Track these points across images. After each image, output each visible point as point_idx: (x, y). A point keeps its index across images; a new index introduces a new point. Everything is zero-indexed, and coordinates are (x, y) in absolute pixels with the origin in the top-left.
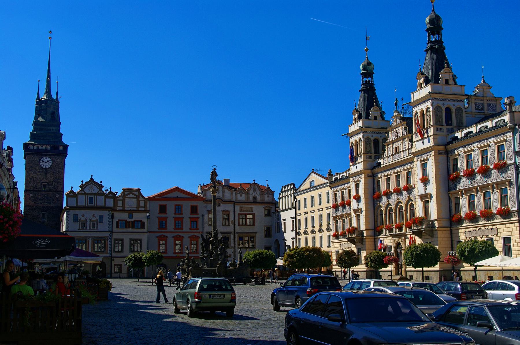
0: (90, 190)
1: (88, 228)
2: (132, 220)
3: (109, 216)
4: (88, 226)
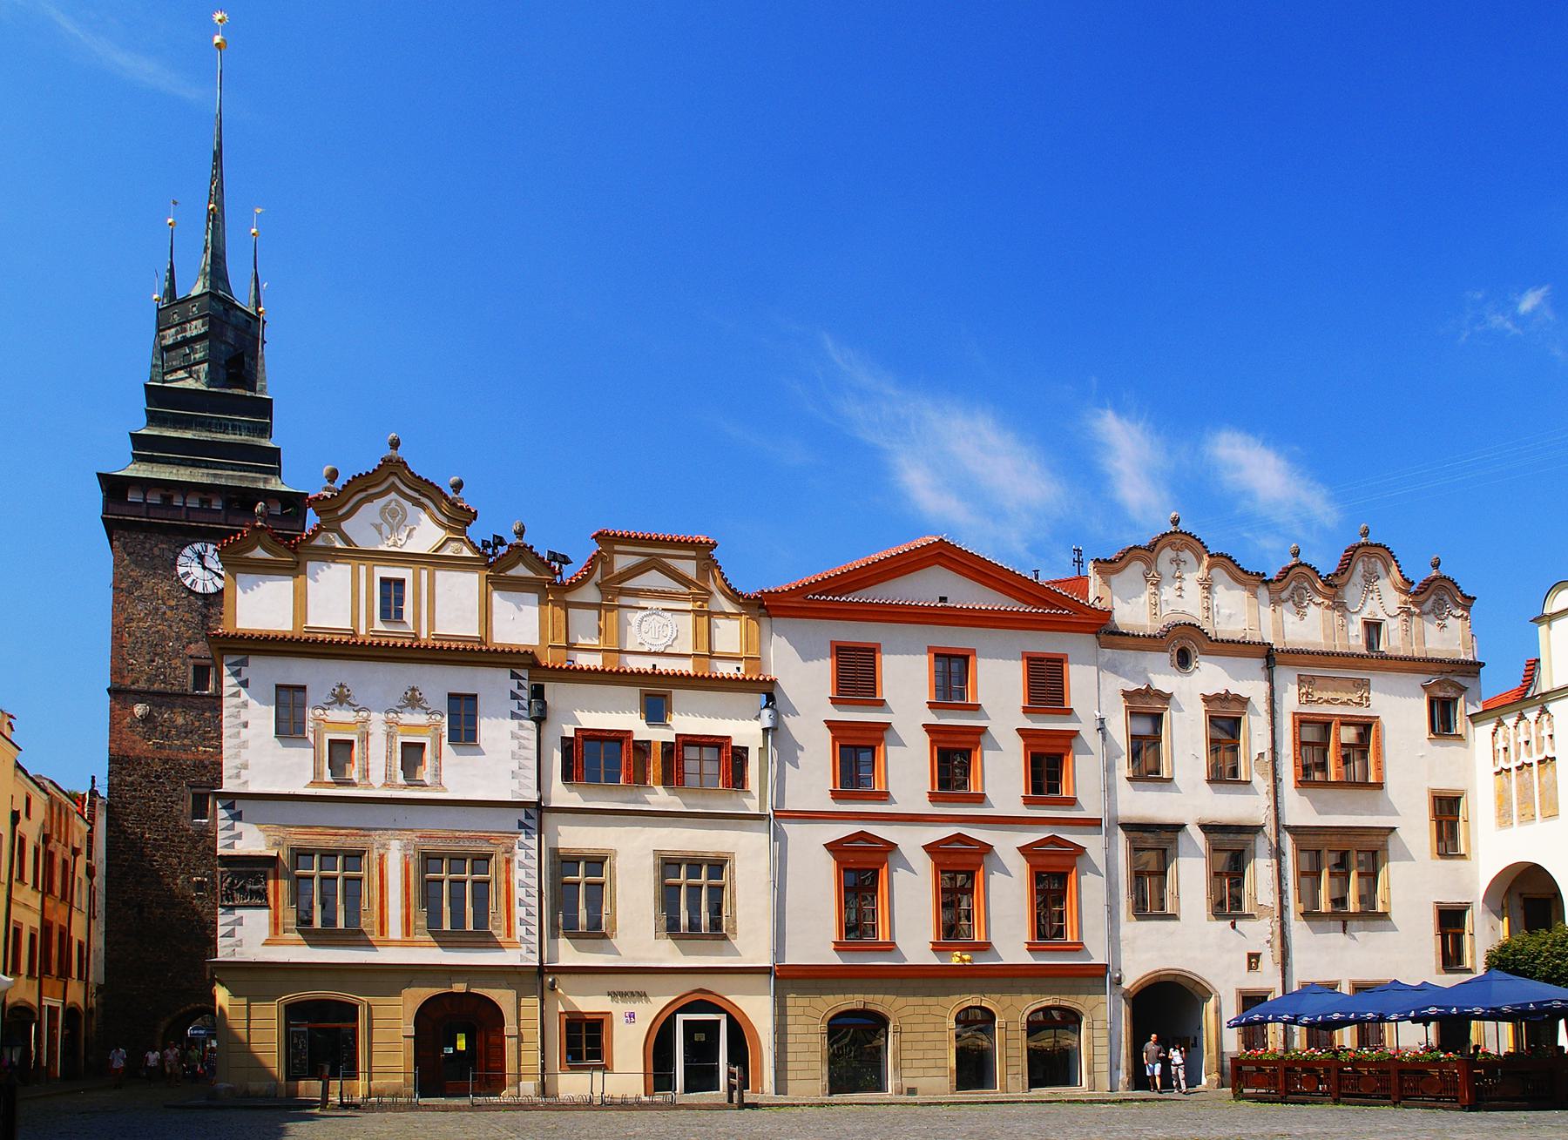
1: (377, 775)
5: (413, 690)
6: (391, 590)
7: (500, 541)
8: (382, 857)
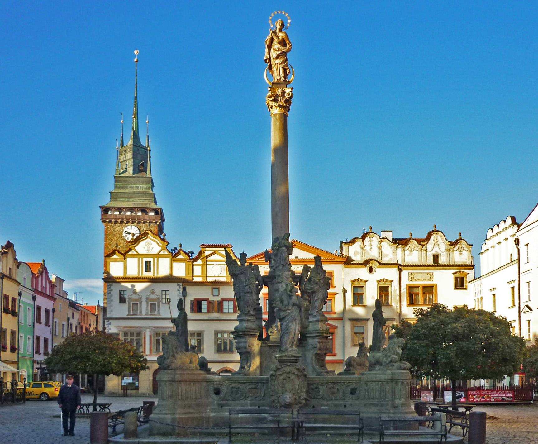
0: (146, 248)
1: (144, 313)
2: (218, 299)
3: (178, 293)
4: (144, 309)
5: (153, 290)
6: (148, 264)
7: (176, 249)
8: (145, 333)
